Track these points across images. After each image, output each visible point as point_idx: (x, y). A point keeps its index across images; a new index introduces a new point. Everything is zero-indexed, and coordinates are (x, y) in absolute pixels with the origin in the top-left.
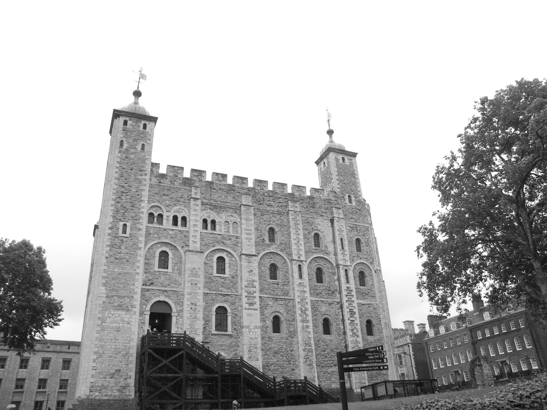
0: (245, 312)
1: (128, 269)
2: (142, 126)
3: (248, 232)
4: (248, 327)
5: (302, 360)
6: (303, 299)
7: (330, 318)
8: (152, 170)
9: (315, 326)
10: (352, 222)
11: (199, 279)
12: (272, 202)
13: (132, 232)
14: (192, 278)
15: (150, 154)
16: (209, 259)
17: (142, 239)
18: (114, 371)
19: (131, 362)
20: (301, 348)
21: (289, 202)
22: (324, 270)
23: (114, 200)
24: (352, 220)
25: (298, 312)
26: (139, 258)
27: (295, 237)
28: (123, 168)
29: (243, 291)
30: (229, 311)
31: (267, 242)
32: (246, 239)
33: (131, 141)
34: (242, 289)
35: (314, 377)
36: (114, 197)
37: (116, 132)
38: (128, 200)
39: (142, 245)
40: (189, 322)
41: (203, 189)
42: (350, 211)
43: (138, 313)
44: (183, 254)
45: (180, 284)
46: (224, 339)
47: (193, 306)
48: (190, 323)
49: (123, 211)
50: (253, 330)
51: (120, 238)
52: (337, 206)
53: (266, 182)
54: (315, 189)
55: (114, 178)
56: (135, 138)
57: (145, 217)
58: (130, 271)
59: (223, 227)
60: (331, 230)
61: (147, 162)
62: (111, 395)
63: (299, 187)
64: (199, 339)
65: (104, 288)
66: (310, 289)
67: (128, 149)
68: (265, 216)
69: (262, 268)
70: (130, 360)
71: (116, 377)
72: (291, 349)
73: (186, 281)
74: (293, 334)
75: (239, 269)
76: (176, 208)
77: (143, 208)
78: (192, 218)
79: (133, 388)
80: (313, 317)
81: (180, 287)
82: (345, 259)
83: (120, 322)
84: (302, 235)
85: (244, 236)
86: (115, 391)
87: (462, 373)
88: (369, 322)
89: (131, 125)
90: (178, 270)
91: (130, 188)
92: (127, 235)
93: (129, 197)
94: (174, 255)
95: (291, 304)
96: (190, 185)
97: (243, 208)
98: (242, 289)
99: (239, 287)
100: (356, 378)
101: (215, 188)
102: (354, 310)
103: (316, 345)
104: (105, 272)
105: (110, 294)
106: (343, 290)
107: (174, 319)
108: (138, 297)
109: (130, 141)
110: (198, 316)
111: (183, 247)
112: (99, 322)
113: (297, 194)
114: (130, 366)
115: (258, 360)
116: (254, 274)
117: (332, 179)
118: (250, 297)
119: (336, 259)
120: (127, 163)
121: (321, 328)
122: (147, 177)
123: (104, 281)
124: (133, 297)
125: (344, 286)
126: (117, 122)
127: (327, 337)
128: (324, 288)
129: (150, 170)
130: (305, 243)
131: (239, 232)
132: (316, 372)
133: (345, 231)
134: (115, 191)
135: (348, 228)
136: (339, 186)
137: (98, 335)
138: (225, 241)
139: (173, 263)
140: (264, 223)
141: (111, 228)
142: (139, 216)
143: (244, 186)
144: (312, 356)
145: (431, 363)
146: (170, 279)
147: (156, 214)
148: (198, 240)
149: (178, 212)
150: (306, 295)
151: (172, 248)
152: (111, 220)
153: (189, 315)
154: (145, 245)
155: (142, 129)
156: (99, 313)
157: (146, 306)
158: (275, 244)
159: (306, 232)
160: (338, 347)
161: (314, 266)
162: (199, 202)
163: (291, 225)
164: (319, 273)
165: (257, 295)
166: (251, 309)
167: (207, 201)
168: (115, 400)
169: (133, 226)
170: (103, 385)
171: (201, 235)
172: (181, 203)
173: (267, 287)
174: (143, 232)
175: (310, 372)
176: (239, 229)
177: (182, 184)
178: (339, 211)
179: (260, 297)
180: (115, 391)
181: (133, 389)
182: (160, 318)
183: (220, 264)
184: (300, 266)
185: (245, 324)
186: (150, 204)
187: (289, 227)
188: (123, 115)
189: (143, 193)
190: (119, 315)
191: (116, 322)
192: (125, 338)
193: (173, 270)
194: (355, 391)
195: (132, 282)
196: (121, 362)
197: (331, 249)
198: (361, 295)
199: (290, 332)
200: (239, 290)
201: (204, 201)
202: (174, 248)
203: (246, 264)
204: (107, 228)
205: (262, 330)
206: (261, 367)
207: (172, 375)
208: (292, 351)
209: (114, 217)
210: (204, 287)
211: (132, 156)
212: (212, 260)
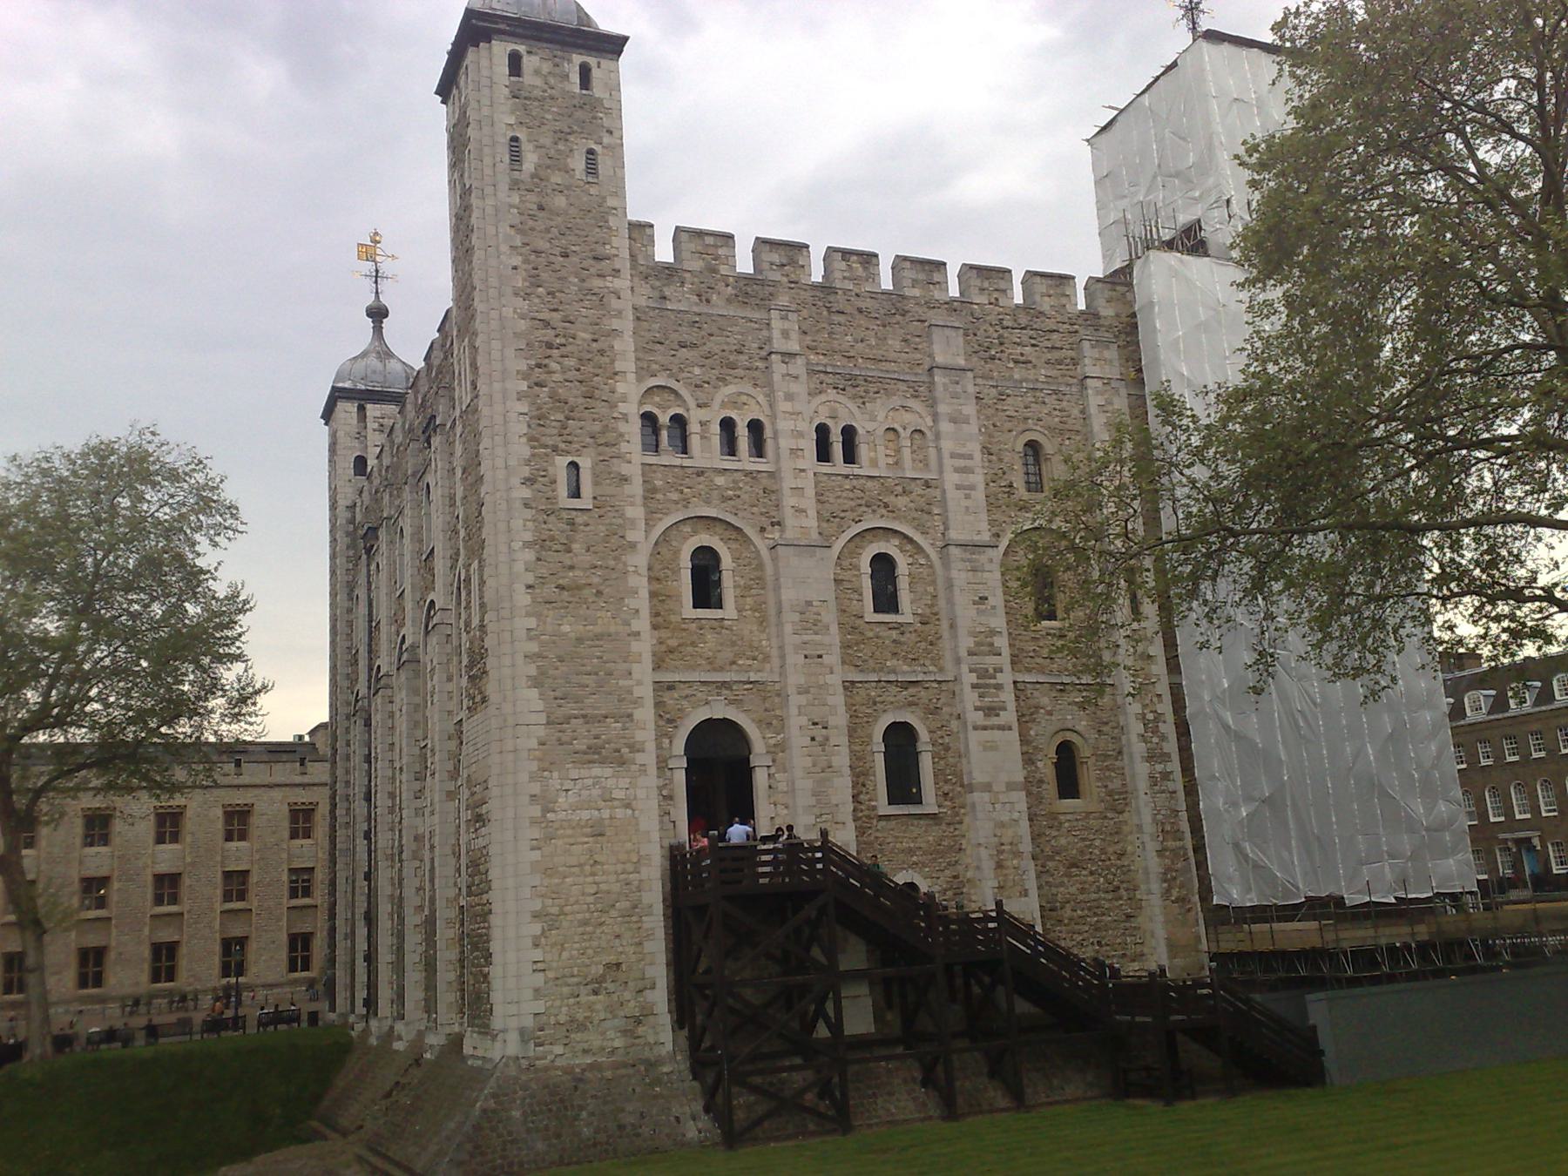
0: (975, 738)
2: (575, 78)
3: (961, 463)
4: (987, 787)
5: (1156, 887)
14: (806, 638)
15: (619, 191)
16: (846, 563)
17: (636, 512)
20: (1152, 847)
21: (1086, 344)
25: (1137, 728)
26: (633, 581)
28: (537, 252)
29: (965, 668)
30: (924, 735)
31: (1021, 492)
32: (958, 487)
34: (958, 661)
35: (1198, 938)
37: (485, 101)
38: (572, 374)
41: (805, 313)
43: (652, 770)
44: (765, 553)
45: (767, 658)
46: (917, 831)
47: (819, 732)
49: (561, 417)
51: (564, 515)
57: (634, 429)
58: (612, 629)
59: (881, 449)
61: (612, 222)
64: (845, 837)
67: (542, 173)
70: (645, 926)
71: (611, 987)
72: (1118, 848)
73: (789, 649)
74: (1119, 801)
75: (941, 594)
77: (624, 399)
78: (784, 425)
81: (768, 666)
85: (951, 478)
87: (1544, 847)
89: (537, 72)
91: (572, 329)
92: (585, 502)
93: (571, 362)
94: (735, 559)
96: (765, 303)
99: (948, 656)
101: (841, 307)
104: (530, 639)
105: (560, 713)
107: (760, 779)
108: (646, 714)
109: (542, 141)
110: (836, 761)
111: (763, 530)
112: (536, 811)
114: (649, 946)
115: (1025, 893)
116: (994, 607)
118: (987, 686)
120: (548, 230)
122: (622, 283)
123: (532, 670)
124: (630, 716)
126: (484, 63)
132: (1201, 922)
140: (1008, 425)
141: (529, 481)
142: (615, 430)
143: (937, 295)
144: (1187, 870)
146: (733, 644)
148: (809, 503)
149: (734, 404)
151: (727, 534)
152: (526, 452)
153: (808, 762)
156: (532, 779)
162: (798, 366)
165: (1006, 678)
167: (824, 360)
168: (616, 1066)
169: (601, 466)
171: (817, 484)
173: (1030, 647)
174: (636, 488)
176: (932, 452)
180: (611, 1034)
181: (664, 1017)
182: (718, 772)
185: (979, 777)
188: (503, 32)
189: (617, 345)
190: (597, 780)
192: (623, 857)
200: (948, 663)
203: (963, 575)
204: (516, 481)
205: (1029, 794)
206: (1037, 914)
208: (1121, 855)
209: (532, 439)
210: (843, 663)
211: (560, 201)
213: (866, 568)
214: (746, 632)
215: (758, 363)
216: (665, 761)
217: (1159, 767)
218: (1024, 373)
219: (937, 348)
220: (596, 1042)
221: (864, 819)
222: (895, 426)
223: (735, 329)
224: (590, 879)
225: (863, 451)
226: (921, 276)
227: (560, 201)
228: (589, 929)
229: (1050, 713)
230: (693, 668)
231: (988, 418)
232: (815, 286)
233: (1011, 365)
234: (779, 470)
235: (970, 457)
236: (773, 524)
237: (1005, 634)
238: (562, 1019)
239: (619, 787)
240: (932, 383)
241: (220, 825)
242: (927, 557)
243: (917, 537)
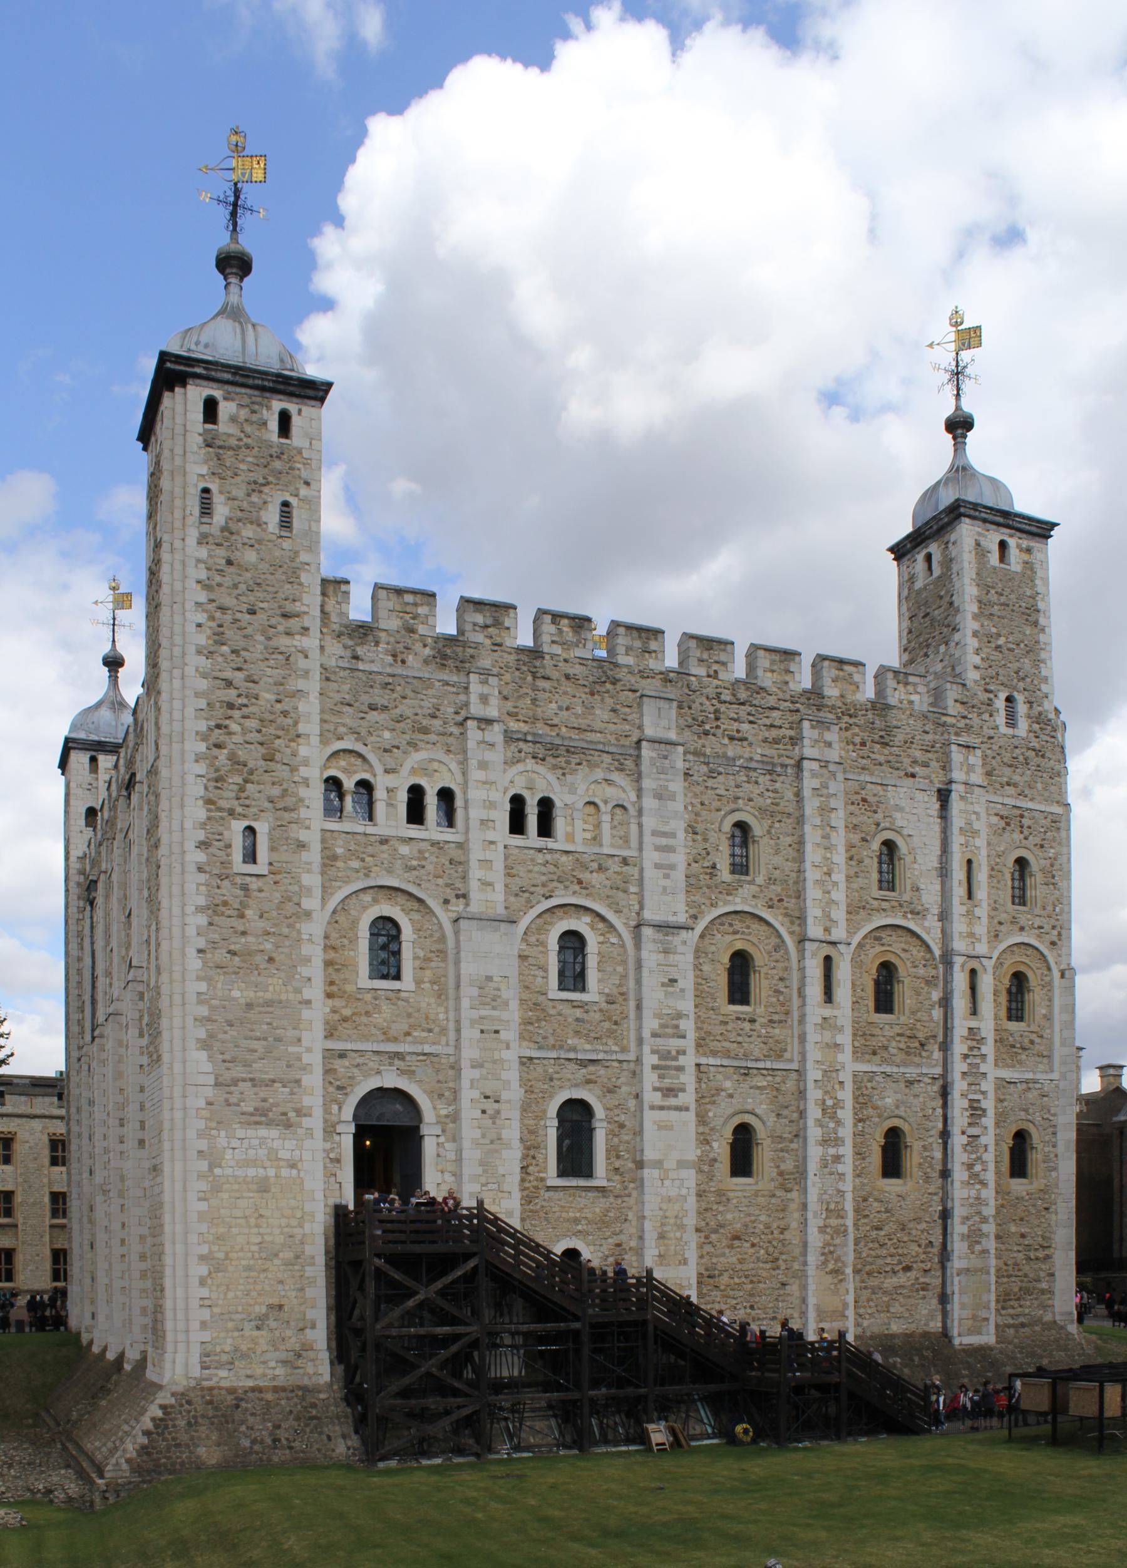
3: (664, 841)
11: (504, 1015)
12: (745, 727)
14: (484, 1013)
16: (532, 939)
18: (264, 1310)
21: (806, 724)
31: (725, 874)
32: (657, 866)
43: (319, 1133)
45: (444, 1031)
48: (480, 1163)
52: (964, 739)
54: (896, 673)
62: (265, 1375)
68: (721, 778)
70: (307, 1275)
71: (273, 1324)
73: (465, 1024)
78: (476, 794)
81: (443, 1040)
83: (268, 1163)
85: (650, 857)
86: (272, 1364)
90: (433, 983)
94: (417, 931)
97: (647, 751)
108: (314, 1080)
111: (446, 902)
113: (831, 691)
117: (955, 629)
131: (634, 843)
138: (585, 876)
139: (416, 958)
146: (409, 1015)
149: (424, 771)
151: (409, 904)
158: (752, 882)
162: (495, 733)
163: (808, 811)
167: (525, 728)
168: (276, 1389)
170: (236, 1350)
171: (506, 858)
172: (432, 737)
178: (972, 760)
179: (698, 1065)
180: (272, 1364)
182: (386, 1143)
187: (800, 821)
190: (263, 1141)
193: (418, 982)
196: (281, 1282)
201: (514, 725)
202: (416, 905)
207: (447, 1329)
212: (542, 944)
213: (553, 944)
214: (424, 1005)
216: (334, 1126)
219: (647, 721)
220: (259, 1371)
222: (597, 800)
223: (430, 692)
224: (256, 1230)
225: (560, 824)
228: (253, 1274)
230: (365, 1038)
231: (696, 795)
232: (520, 650)
233: (726, 741)
234: (467, 840)
235: (673, 835)
236: (457, 896)
238: (227, 1349)
239: (286, 1148)
240: (639, 756)
242: (620, 936)
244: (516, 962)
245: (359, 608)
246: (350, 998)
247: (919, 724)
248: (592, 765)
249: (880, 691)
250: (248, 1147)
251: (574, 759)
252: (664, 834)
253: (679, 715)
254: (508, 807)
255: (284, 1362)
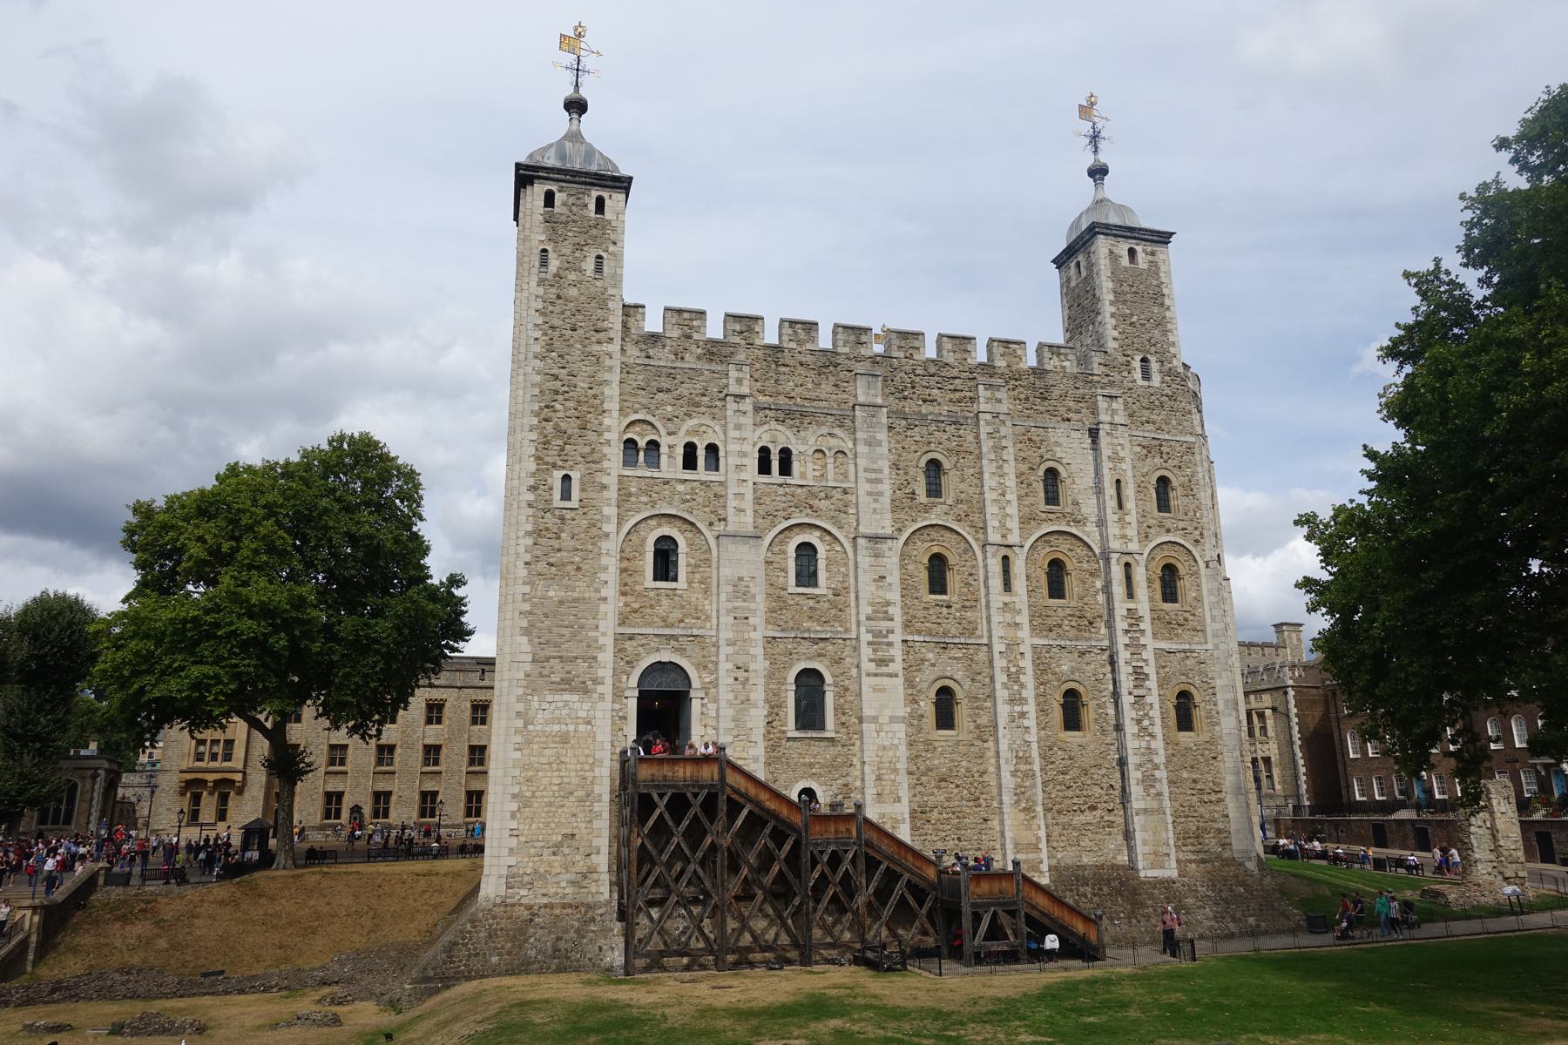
0: (867, 682)
1: (581, 588)
2: (592, 207)
3: (873, 476)
4: (875, 719)
5: (1007, 798)
6: (1012, 645)
7: (1081, 689)
8: (625, 326)
9: (1043, 711)
10: (1149, 432)
11: (753, 606)
12: (936, 391)
13: (584, 495)
15: (617, 281)
16: (776, 549)
17: (610, 511)
19: (598, 816)
22: (1069, 566)
23: (537, 415)
24: (1151, 427)
26: (604, 561)
27: (994, 484)
28: (552, 327)
29: (863, 629)
30: (828, 679)
31: (922, 498)
32: (869, 494)
33: (567, 251)
35: (1038, 838)
36: (536, 407)
38: (571, 413)
39: (610, 528)
40: (731, 712)
42: (1145, 402)
43: (609, 697)
45: (708, 618)
46: (816, 750)
47: (741, 674)
50: (886, 728)
53: (918, 335)
55: (531, 355)
56: (577, 240)
57: (615, 452)
59: (810, 466)
60: (1091, 458)
63: (1006, 343)
65: (525, 639)
66: (1032, 616)
67: (562, 273)
69: (910, 567)
71: (566, 851)
72: (981, 768)
73: (722, 612)
76: (691, 423)
77: (609, 429)
78: (733, 447)
79: (605, 878)
80: (1037, 688)
82: (1124, 537)
84: (1012, 476)
85: (864, 487)
88: (1184, 696)
92: (574, 503)
93: (571, 404)
94: (690, 545)
95: (982, 655)
96: (725, 359)
97: (859, 412)
98: (858, 624)
100: (1145, 843)
101: (787, 361)
102: (1146, 670)
103: (1043, 757)
104: (525, 601)
105: (542, 654)
106: (1118, 618)
107: (696, 706)
108: (607, 657)
110: (753, 696)
111: (711, 524)
112: (520, 723)
113: (1000, 363)
114: (596, 824)
115: (898, 800)
117: (1098, 313)
119: (1101, 535)
121: (1057, 715)
122: (615, 348)
123: (525, 624)
124: (595, 658)
125: (1121, 607)
127: (1073, 737)
128: (1068, 611)
129: (618, 326)
130: (1020, 498)
133: (1128, 460)
134: (536, 391)
135: (1138, 449)
136: (1115, 334)
137: (518, 755)
138: (815, 503)
141: (533, 488)
143: (863, 351)
144: (1034, 786)
145: (1343, 742)
146: (683, 607)
147: (642, 443)
148: (748, 504)
150: (1020, 634)
152: (533, 467)
153: (731, 696)
154: (619, 524)
155: (593, 214)
156: (518, 701)
157: (628, 676)
159: (1024, 467)
160: (1100, 761)
161: (1044, 556)
162: (747, 405)
163: (984, 450)
164: (1056, 570)
165: (896, 638)
166: (882, 675)
168: (564, 906)
172: (703, 409)
174: (612, 494)
175: (1029, 827)
177: (700, 355)
180: (564, 884)
181: (605, 878)
183: (805, 560)
184: (1005, 558)
185: (867, 712)
186: (626, 416)
187: (980, 457)
189: (607, 391)
190: (566, 703)
191: (559, 721)
192: (582, 759)
193: (690, 583)
194: (1142, 874)
195: (591, 622)
197: (1089, 508)
198: (1167, 627)
199: (978, 727)
208: (982, 774)
209: (538, 458)
211: (573, 292)
212: (784, 553)
215: (717, 401)
217: (1018, 709)
218: (931, 409)
219: (859, 391)
221: (774, 744)
225: (796, 466)
226: (852, 338)
227: (573, 292)
229: (933, 665)
230: (649, 624)
237: (899, 604)
239: (581, 706)
241: (468, 713)
243: (834, 531)
244: (762, 566)
245: (653, 322)
246: (639, 595)
247: (1071, 382)
248: (819, 424)
249: (1040, 361)
250: (555, 708)
251: (806, 421)
252: (874, 471)
253: (885, 386)
254: (757, 455)
255: (573, 883)
